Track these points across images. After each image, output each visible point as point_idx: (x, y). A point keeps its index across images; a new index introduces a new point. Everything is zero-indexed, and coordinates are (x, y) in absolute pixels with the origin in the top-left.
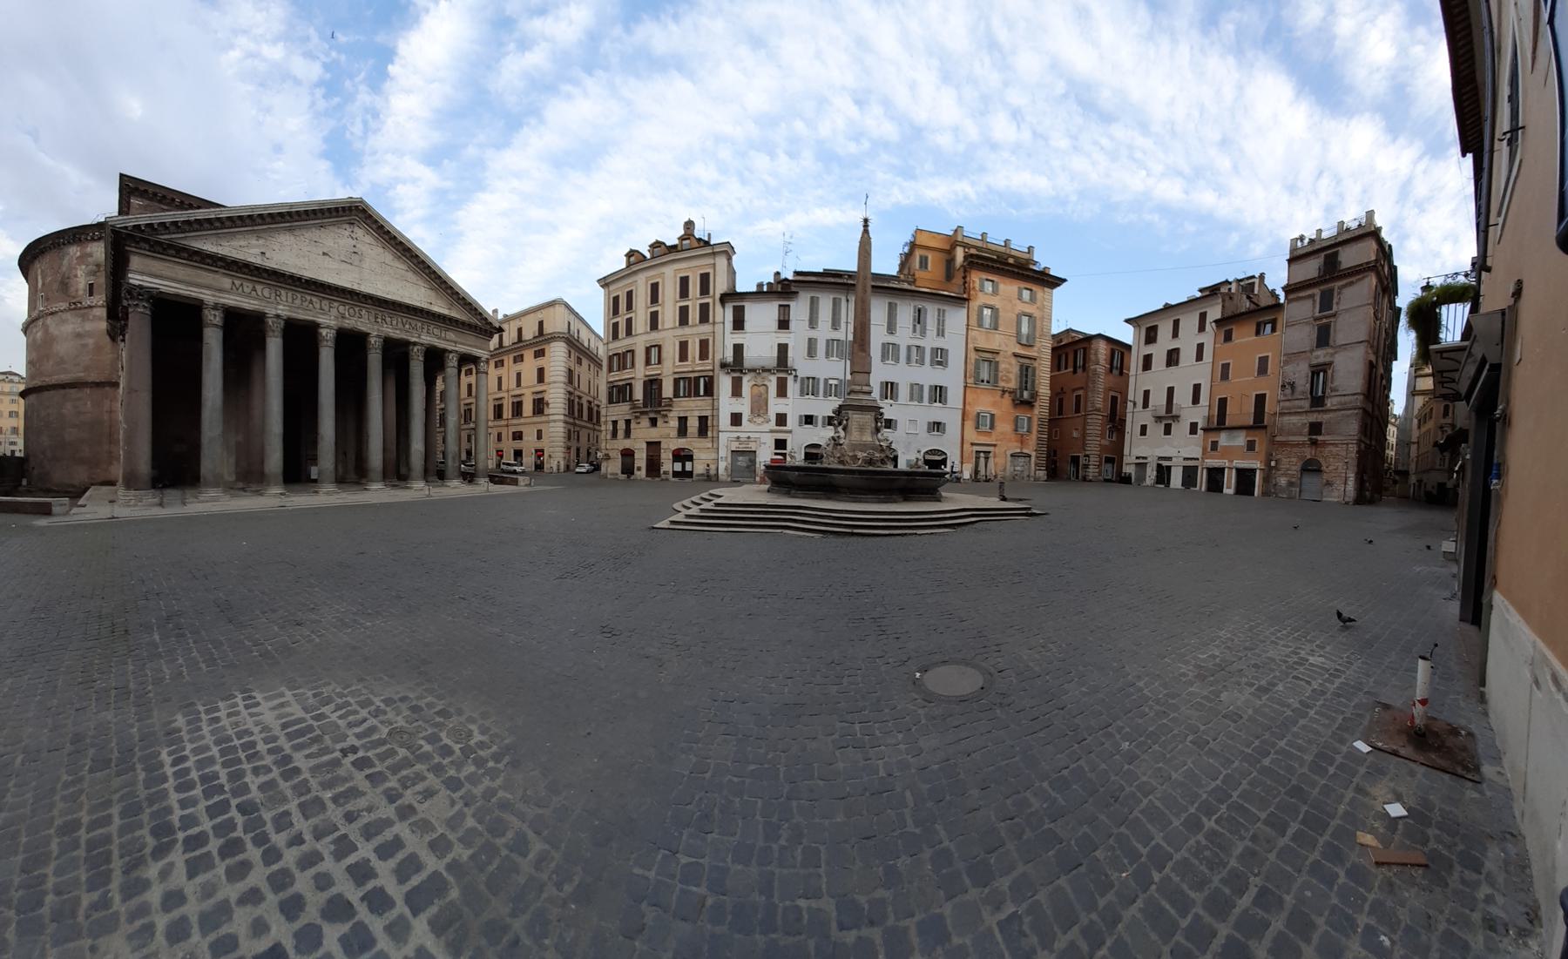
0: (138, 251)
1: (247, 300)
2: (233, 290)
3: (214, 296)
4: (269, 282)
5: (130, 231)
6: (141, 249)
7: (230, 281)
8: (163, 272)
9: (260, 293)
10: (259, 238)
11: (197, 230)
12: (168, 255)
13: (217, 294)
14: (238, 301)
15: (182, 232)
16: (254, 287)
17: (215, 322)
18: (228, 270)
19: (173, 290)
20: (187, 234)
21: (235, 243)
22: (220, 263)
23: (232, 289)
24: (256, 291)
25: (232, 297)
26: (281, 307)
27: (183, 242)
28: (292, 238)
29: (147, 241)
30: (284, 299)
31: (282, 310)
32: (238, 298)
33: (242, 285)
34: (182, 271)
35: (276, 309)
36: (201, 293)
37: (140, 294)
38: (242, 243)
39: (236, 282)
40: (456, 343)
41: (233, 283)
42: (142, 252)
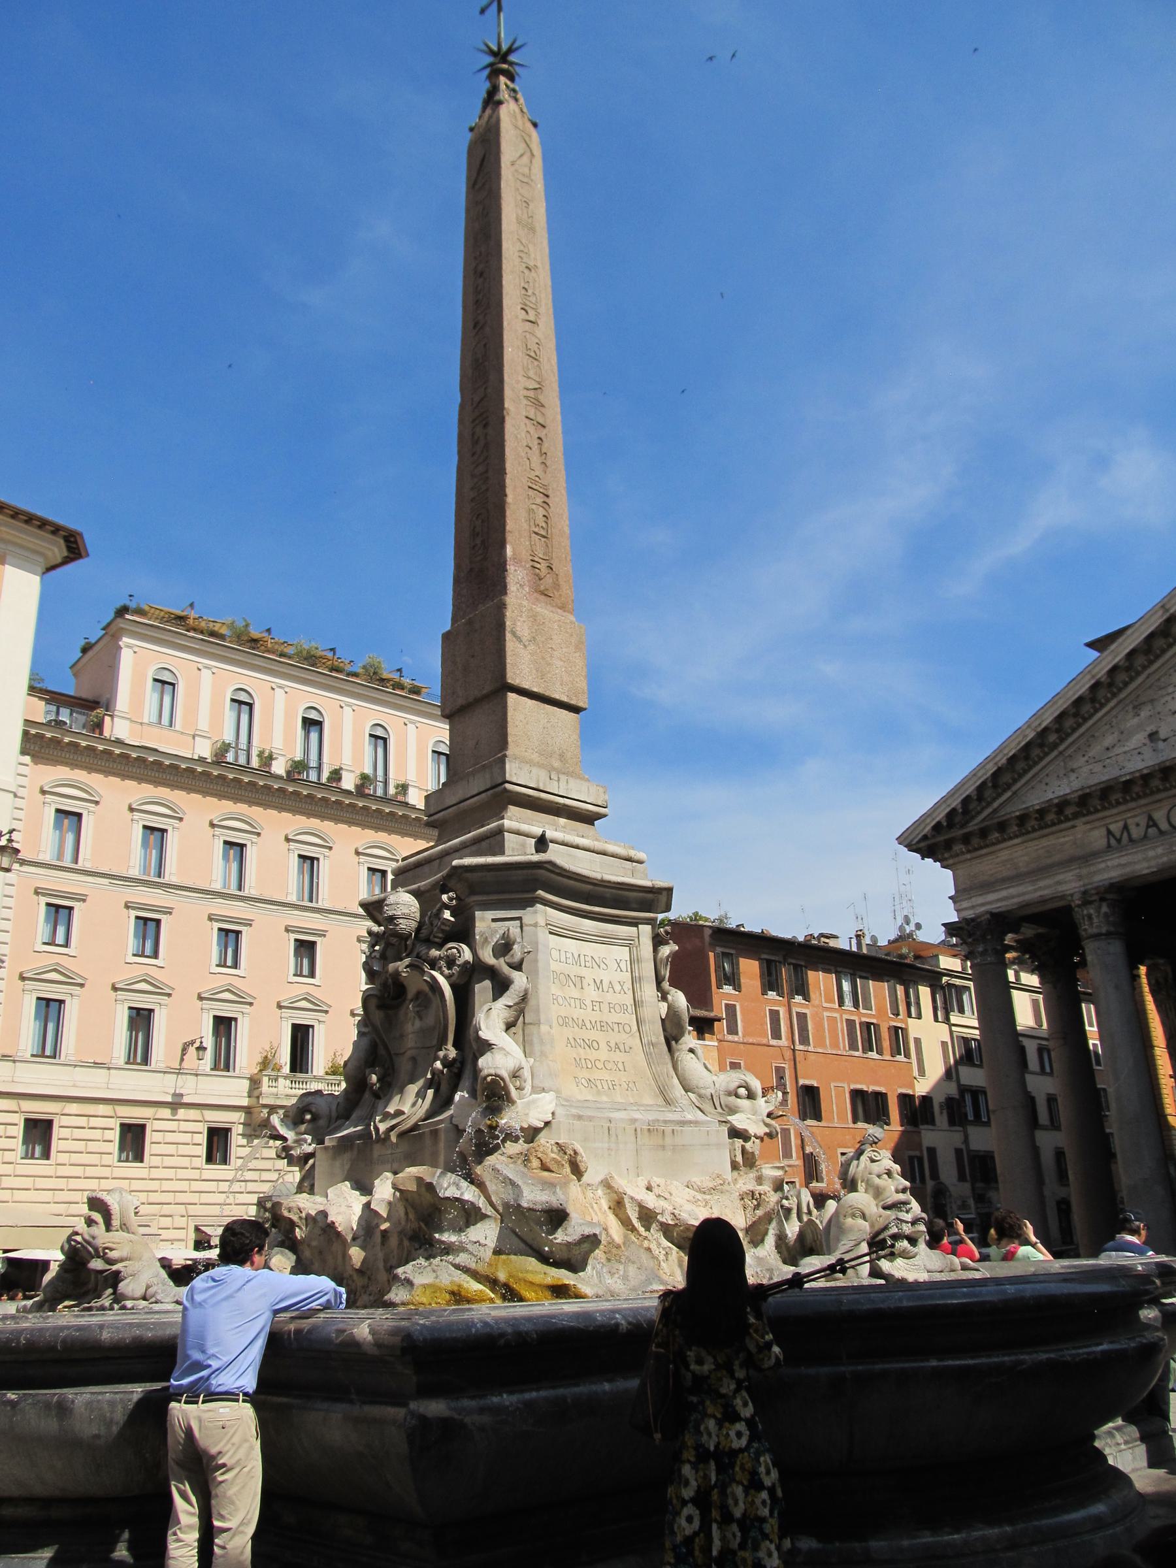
0: (956, 860)
1: (1140, 856)
2: (1117, 842)
3: (1080, 878)
5: (934, 836)
6: (957, 855)
7: (1103, 831)
9: (1164, 826)
10: (1137, 708)
11: (1025, 772)
12: (994, 844)
13: (1084, 871)
14: (1124, 865)
15: (1005, 791)
16: (1150, 818)
17: (1095, 931)
19: (1015, 900)
20: (1014, 788)
21: (1096, 750)
23: (1109, 846)
24: (1155, 825)
25: (1109, 863)
32: (1123, 860)
33: (1126, 827)
36: (1059, 883)
37: (970, 936)
38: (1109, 740)
39: (1112, 827)
41: (1109, 832)
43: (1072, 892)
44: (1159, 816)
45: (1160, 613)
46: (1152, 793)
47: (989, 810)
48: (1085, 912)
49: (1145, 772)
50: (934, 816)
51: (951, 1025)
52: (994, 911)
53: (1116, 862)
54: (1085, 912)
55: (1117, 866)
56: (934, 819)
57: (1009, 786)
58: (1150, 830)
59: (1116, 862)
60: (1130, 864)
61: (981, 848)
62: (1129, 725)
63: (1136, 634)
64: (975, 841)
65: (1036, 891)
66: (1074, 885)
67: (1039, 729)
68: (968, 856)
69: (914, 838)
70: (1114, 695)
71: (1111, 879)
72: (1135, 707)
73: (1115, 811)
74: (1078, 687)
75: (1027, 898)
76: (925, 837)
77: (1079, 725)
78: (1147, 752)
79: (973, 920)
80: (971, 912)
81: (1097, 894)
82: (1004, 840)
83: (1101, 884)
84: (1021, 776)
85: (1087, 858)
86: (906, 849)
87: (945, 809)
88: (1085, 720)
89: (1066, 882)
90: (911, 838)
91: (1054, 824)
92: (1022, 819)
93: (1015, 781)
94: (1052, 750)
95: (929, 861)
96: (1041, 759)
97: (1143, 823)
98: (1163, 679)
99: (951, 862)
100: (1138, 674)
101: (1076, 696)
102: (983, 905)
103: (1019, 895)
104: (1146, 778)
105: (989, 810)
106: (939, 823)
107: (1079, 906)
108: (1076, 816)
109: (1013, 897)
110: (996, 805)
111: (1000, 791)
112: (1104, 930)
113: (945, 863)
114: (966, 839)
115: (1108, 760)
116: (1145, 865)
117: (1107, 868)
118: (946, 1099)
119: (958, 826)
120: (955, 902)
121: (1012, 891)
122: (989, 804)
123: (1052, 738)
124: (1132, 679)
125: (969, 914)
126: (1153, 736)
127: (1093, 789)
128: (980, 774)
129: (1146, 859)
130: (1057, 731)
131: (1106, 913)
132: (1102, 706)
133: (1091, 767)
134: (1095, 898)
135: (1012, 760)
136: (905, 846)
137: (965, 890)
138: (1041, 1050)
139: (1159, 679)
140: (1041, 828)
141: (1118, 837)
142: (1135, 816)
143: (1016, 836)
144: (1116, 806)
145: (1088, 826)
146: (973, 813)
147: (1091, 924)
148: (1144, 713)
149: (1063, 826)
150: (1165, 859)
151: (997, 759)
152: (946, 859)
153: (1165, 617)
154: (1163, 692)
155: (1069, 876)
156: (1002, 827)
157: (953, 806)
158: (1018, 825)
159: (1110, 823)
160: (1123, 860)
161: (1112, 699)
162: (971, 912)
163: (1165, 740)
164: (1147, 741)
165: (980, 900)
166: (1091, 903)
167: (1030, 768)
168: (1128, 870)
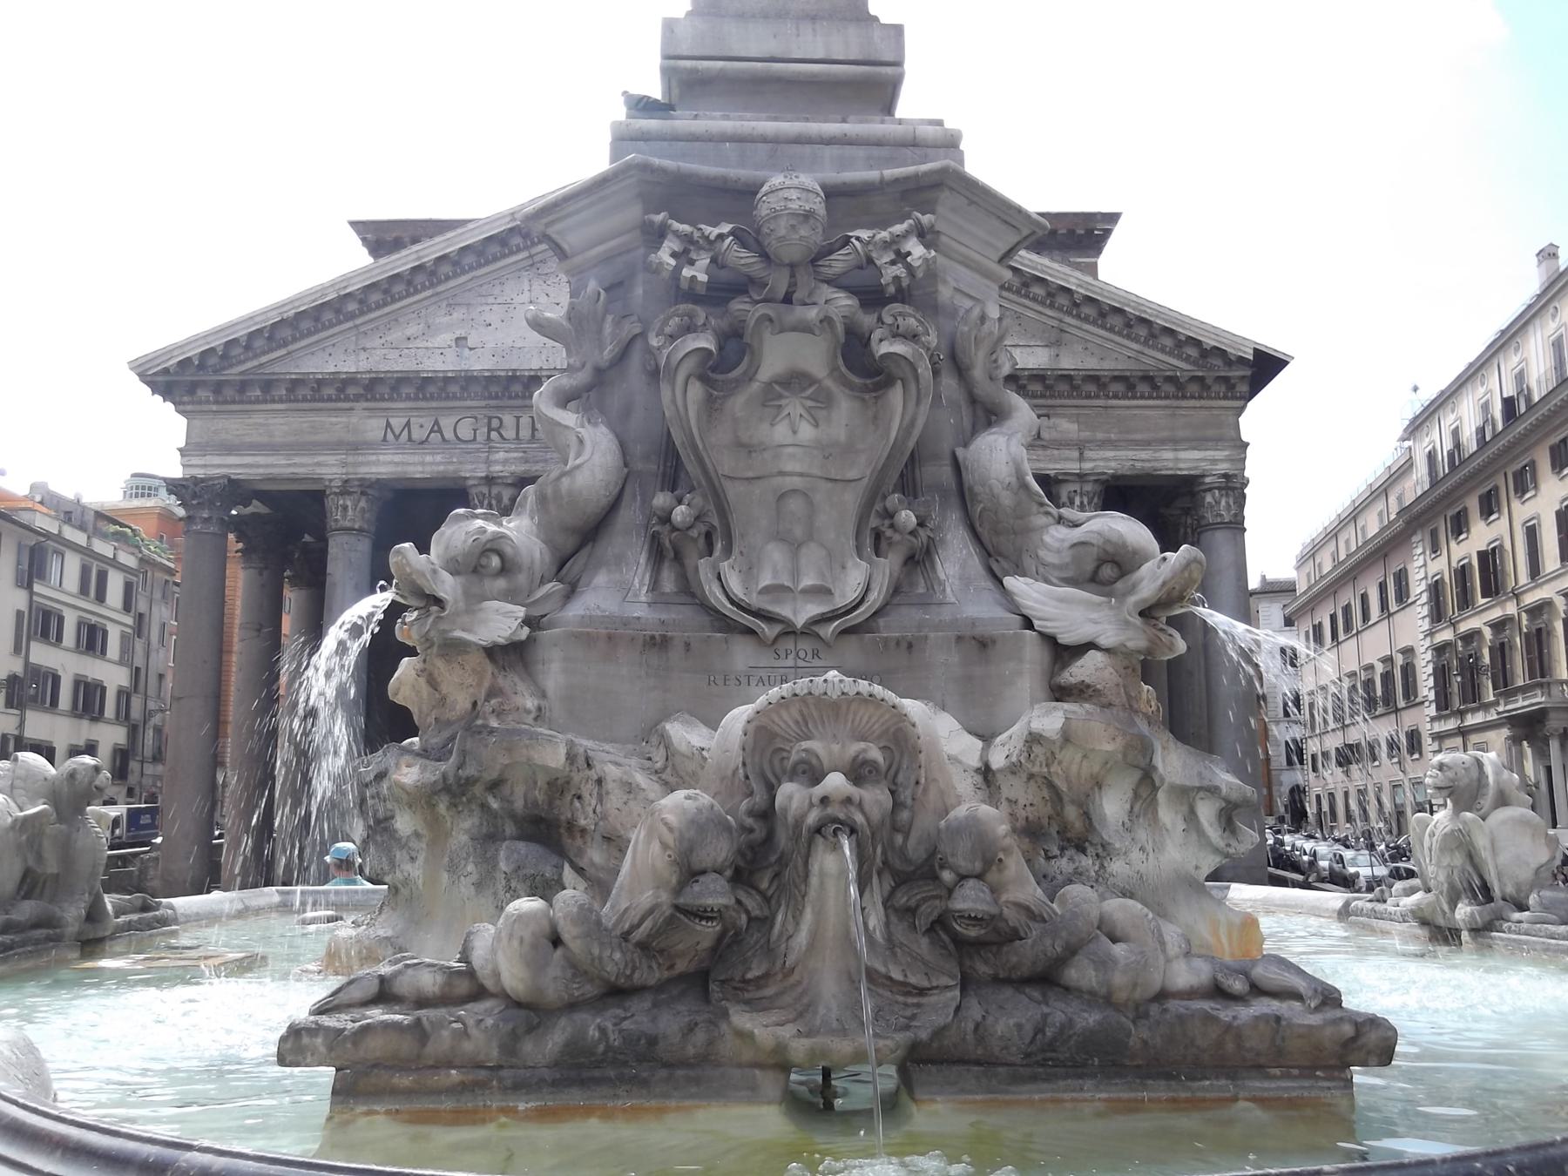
0: (198, 408)
1: (416, 459)
3: (344, 464)
4: (469, 403)
5: (176, 373)
6: (200, 403)
8: (247, 439)
9: (449, 435)
11: (310, 333)
12: (250, 402)
13: (350, 459)
14: (397, 464)
15: (279, 347)
16: (436, 423)
17: (347, 524)
18: (374, 399)
19: (261, 471)
20: (291, 348)
21: (396, 335)
22: (351, 391)
23: (385, 439)
24: (440, 431)
25: (381, 457)
26: (501, 455)
27: (277, 370)
28: (537, 284)
29: (203, 384)
30: (509, 433)
31: (505, 462)
32: (397, 458)
33: (408, 424)
34: (279, 423)
35: (488, 462)
36: (319, 464)
37: (195, 496)
38: (412, 330)
39: (392, 421)
40: (1081, 447)
41: (388, 425)
42: (205, 407)
43: (330, 477)
44: (447, 423)
45: (508, 219)
46: (447, 398)
47: (255, 363)
48: (341, 502)
49: (450, 375)
50: (186, 349)
51: (32, 593)
52: (233, 477)
53: (388, 458)
54: (341, 502)
55: (390, 463)
56: (184, 353)
57: (285, 344)
58: (433, 435)
59: (388, 458)
60: (403, 463)
61: (234, 402)
62: (437, 321)
63: (476, 232)
64: (229, 393)
65: (289, 465)
66: (335, 470)
67: (343, 293)
68: (214, 408)
69: (150, 369)
70: (432, 285)
71: (379, 473)
72: (449, 305)
73: (402, 405)
74: (399, 263)
75: (275, 471)
76: (166, 371)
77: (385, 304)
78: (450, 355)
79: (202, 480)
80: (202, 471)
81: (360, 486)
82: (265, 402)
83: (368, 476)
84: (303, 337)
85: (356, 447)
86: (137, 378)
87: (200, 346)
88: (394, 301)
89: (327, 465)
90: (147, 366)
91: (330, 399)
92: (295, 384)
93: (295, 340)
94: (347, 320)
95: (158, 398)
96: (332, 325)
97: (429, 424)
98: (485, 287)
99: (189, 408)
100: (464, 272)
101: (396, 272)
102: (219, 466)
103: (267, 466)
104: (447, 380)
105: (255, 363)
106: (189, 359)
107: (335, 493)
108: (357, 398)
109: (259, 466)
110: (264, 359)
111: (274, 345)
112: (356, 527)
113: (182, 407)
114: (218, 388)
115: (406, 351)
116: (420, 469)
117: (377, 463)
118: (9, 676)
119: (210, 370)
120: (182, 455)
121: (261, 460)
122: (256, 356)
123: (352, 306)
124: (456, 275)
125: (200, 473)
126: (460, 341)
127: (389, 375)
128: (257, 319)
129: (423, 464)
130: (361, 302)
131: (363, 510)
132: (417, 292)
133: (384, 351)
134: (358, 490)
135: (300, 316)
136: (139, 375)
137: (198, 444)
138: (123, 636)
139: (481, 285)
140: (314, 400)
141: (397, 433)
142: (421, 417)
143: (281, 401)
144: (405, 401)
145: (366, 413)
146: (234, 361)
147: (344, 517)
148: (457, 315)
149: (340, 405)
150: (441, 468)
151: (285, 309)
152: (184, 403)
153: (509, 226)
154: (483, 300)
155: (331, 459)
156: (268, 385)
157: (212, 345)
158: (287, 389)
159: (392, 417)
160: (397, 458)
161: (429, 289)
162: (202, 471)
163: (471, 349)
164: (453, 344)
165: (217, 460)
166: (350, 493)
167: (317, 331)
168: (399, 469)
